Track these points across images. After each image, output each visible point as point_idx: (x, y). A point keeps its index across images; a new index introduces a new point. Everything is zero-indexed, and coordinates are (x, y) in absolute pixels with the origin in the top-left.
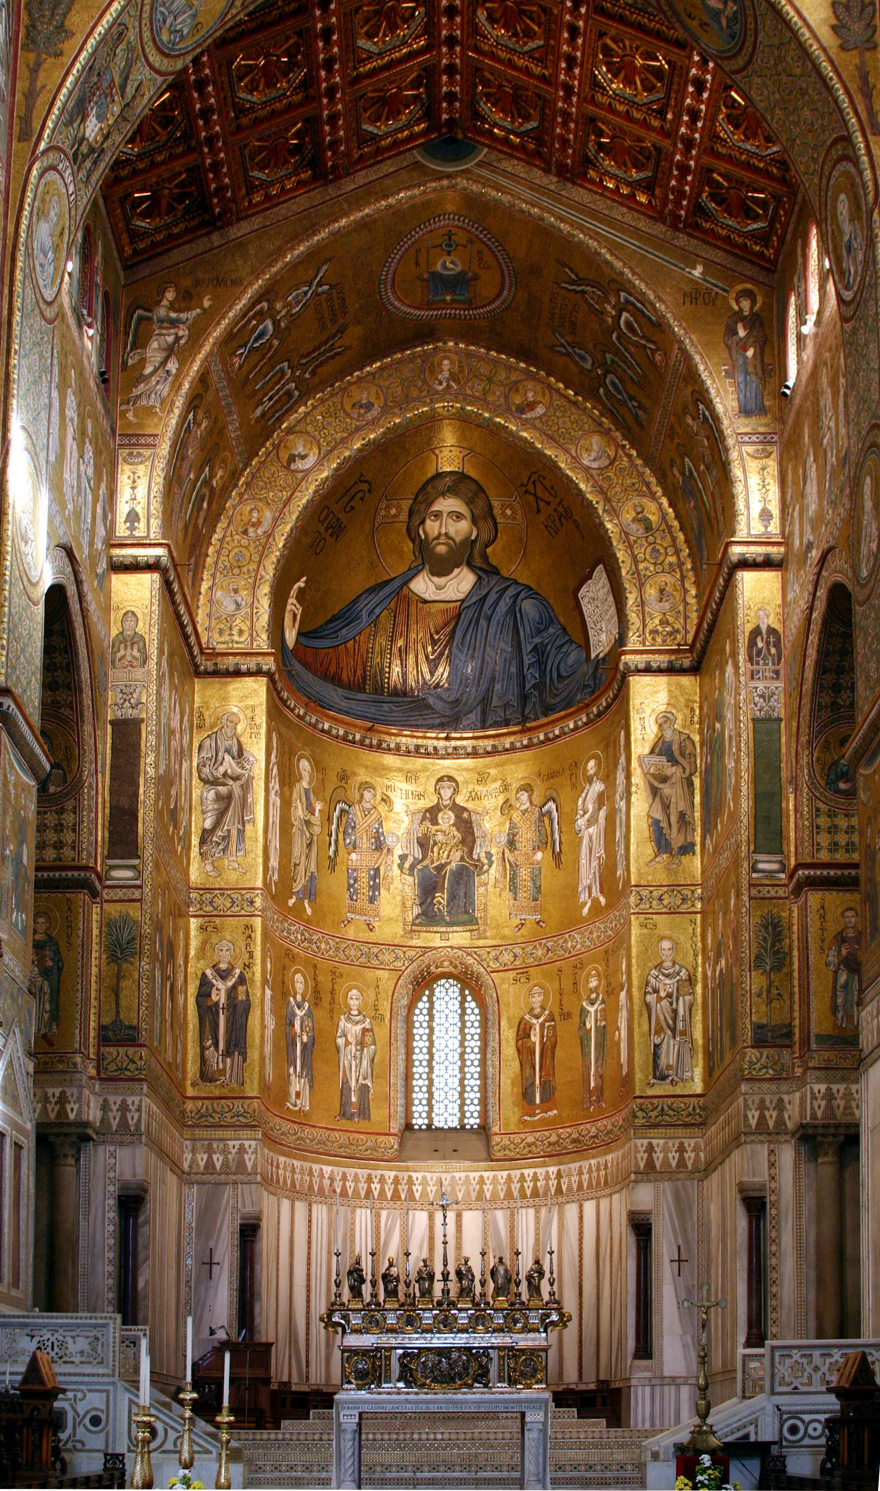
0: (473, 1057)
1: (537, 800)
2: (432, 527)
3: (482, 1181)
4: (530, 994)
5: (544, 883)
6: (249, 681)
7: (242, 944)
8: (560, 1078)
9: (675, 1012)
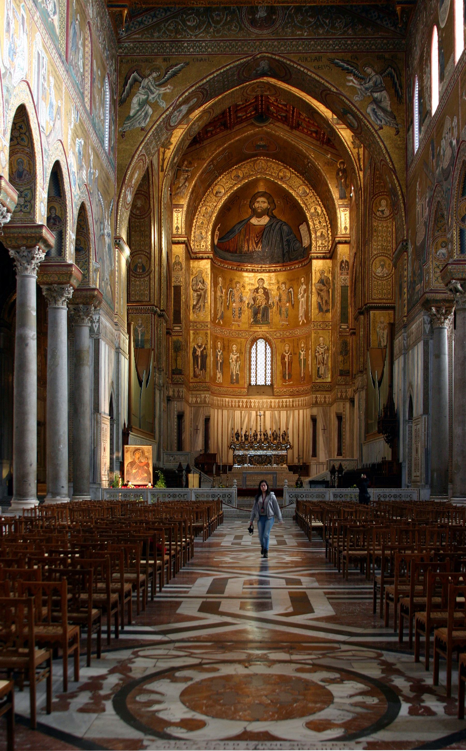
0: (269, 363)
1: (287, 287)
2: (256, 205)
3: (271, 402)
4: (285, 346)
5: (289, 312)
6: (204, 262)
7: (205, 338)
8: (293, 372)
9: (324, 358)
